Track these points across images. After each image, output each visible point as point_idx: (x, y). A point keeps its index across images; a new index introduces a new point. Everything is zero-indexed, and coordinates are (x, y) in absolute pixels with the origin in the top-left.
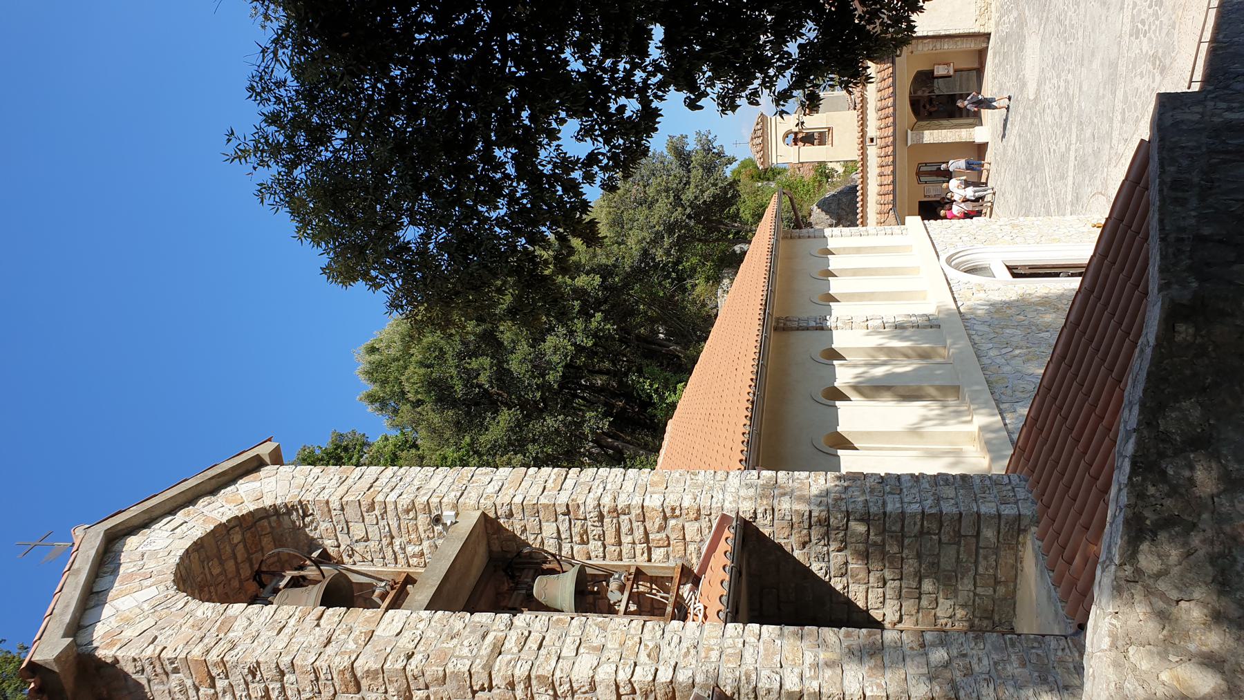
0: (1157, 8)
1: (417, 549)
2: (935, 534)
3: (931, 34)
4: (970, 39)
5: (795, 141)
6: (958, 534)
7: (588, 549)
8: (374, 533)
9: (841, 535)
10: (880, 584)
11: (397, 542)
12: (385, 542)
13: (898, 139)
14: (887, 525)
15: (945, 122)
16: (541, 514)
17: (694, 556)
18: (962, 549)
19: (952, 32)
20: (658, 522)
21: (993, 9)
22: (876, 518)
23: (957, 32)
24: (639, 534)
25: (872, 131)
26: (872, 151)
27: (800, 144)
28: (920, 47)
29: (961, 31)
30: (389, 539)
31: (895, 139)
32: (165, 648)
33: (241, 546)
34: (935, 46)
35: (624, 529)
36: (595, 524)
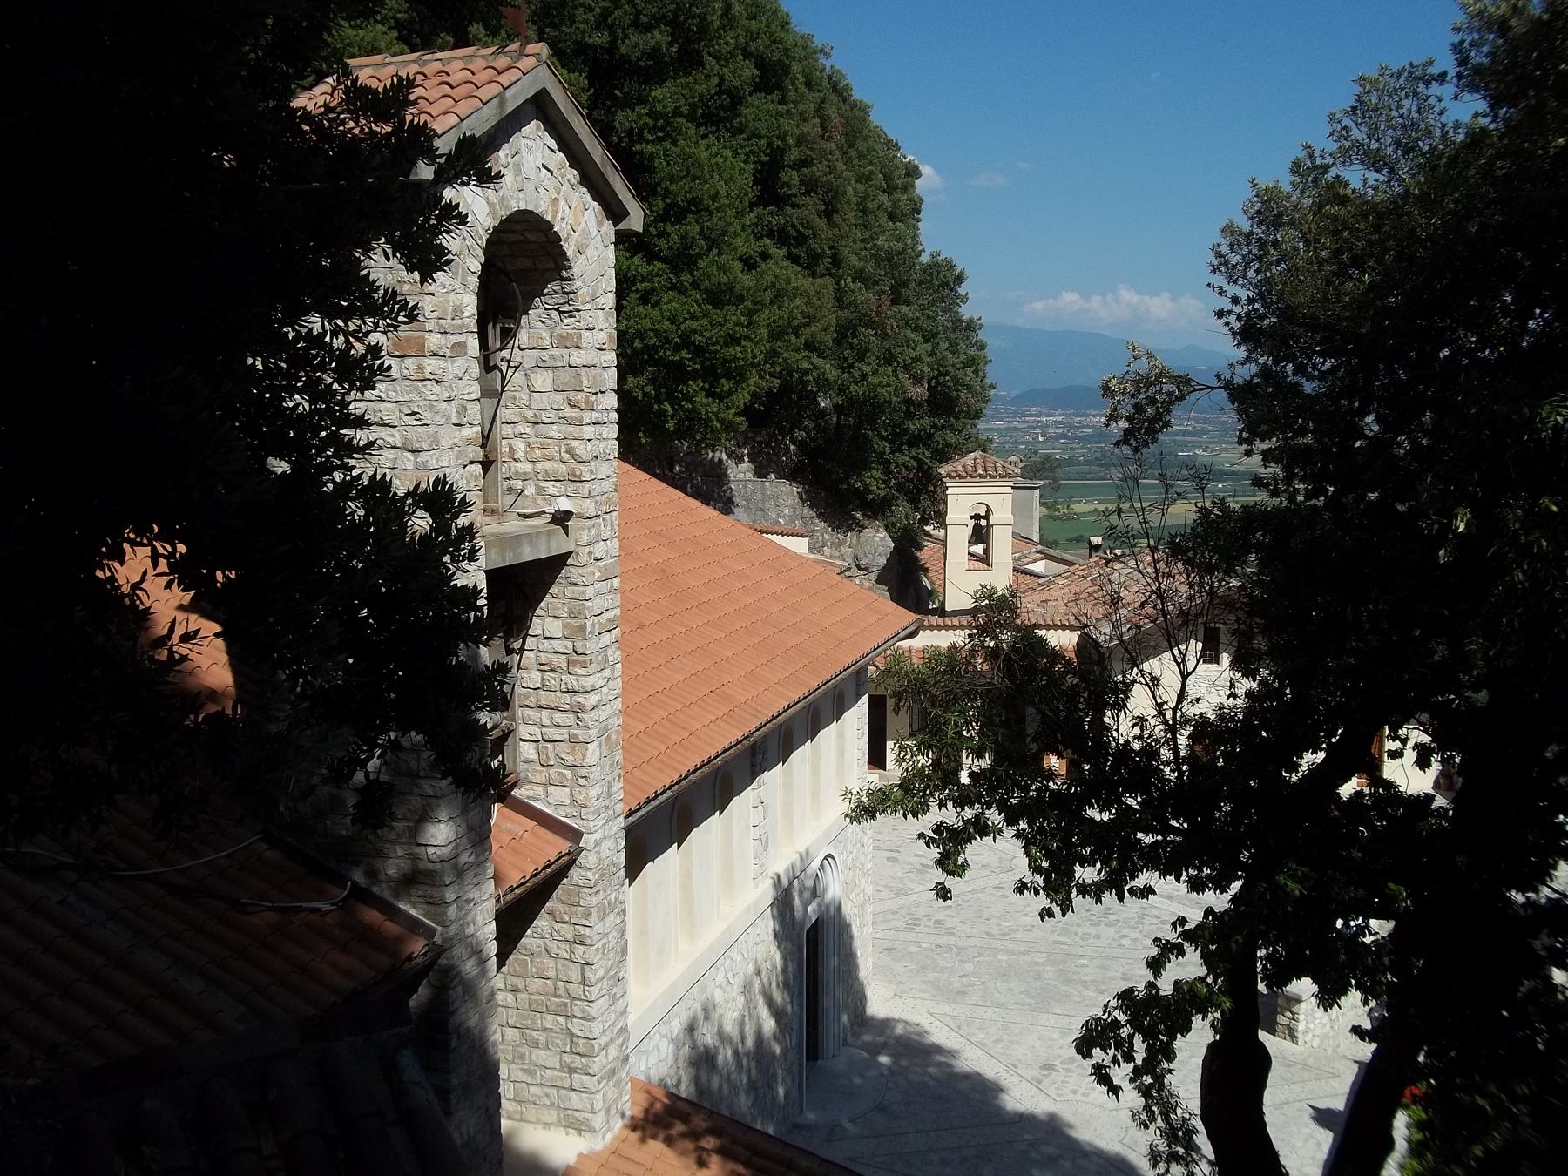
1: (520, 455)
2: (571, 1048)
5: (976, 517)
6: (572, 1071)
7: (531, 669)
8: (540, 402)
9: (565, 954)
10: (509, 987)
11: (528, 429)
12: (529, 414)
14: (579, 1003)
16: (572, 621)
17: (530, 793)
18: (556, 1073)
20: (570, 759)
22: (586, 993)
24: (552, 733)
30: (533, 420)
32: (433, 294)
33: (521, 238)
35: (558, 717)
36: (563, 683)
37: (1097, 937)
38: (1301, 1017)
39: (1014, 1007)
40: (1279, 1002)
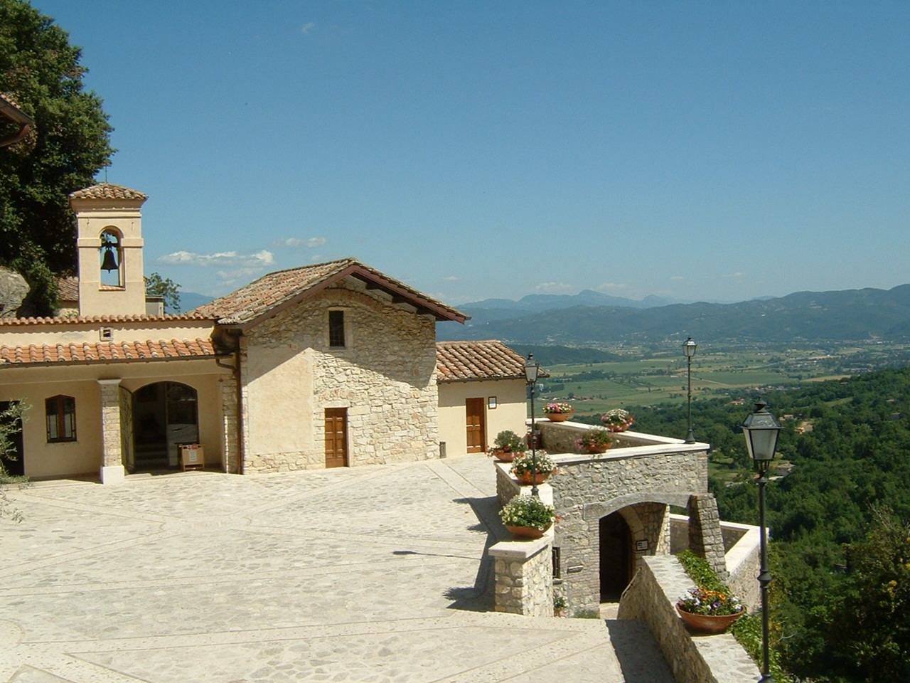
0: (314, 674)
3: (244, 401)
4: (236, 451)
13: (106, 365)
15: (130, 428)
19: (245, 428)
21: (271, 475)
23: (246, 434)
25: (121, 337)
26: (92, 337)
27: (104, 249)
28: (227, 390)
29: (246, 439)
31: (108, 362)
34: (228, 408)
37: (268, 565)
38: (524, 580)
39: (179, 632)
40: (497, 568)
